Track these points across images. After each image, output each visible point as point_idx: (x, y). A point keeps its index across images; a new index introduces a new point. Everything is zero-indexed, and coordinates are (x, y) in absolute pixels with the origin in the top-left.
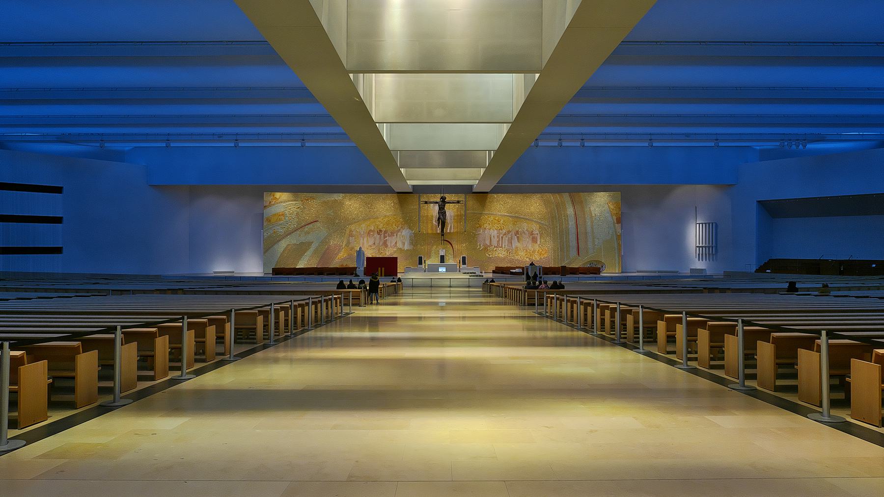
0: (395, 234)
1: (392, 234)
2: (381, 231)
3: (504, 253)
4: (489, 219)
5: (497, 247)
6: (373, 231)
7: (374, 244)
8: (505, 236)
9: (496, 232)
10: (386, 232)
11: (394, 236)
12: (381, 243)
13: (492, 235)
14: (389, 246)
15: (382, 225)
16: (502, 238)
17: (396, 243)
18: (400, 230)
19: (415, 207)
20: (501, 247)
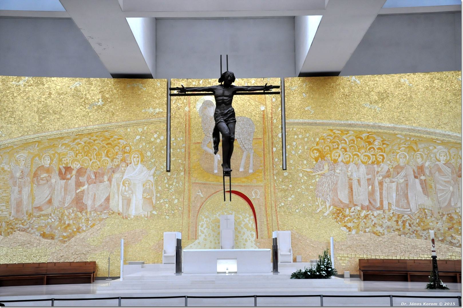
0: (106, 178)
1: (98, 176)
2: (68, 169)
3: (389, 223)
4: (344, 137)
5: (368, 207)
6: (48, 171)
7: (50, 202)
8: (387, 180)
9: (363, 169)
10: (81, 172)
11: (101, 182)
12: (69, 199)
13: (355, 176)
14: (89, 210)
15: (72, 153)
16: (381, 183)
17: (108, 199)
18: (118, 166)
19: (157, 110)
20: (378, 209)
